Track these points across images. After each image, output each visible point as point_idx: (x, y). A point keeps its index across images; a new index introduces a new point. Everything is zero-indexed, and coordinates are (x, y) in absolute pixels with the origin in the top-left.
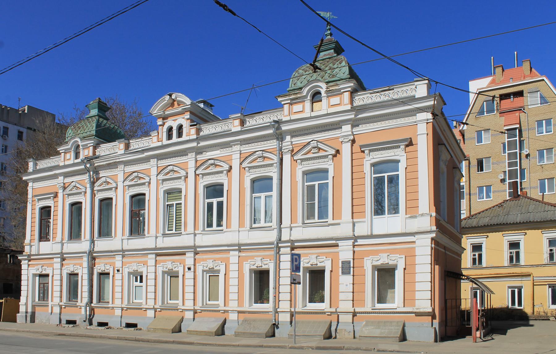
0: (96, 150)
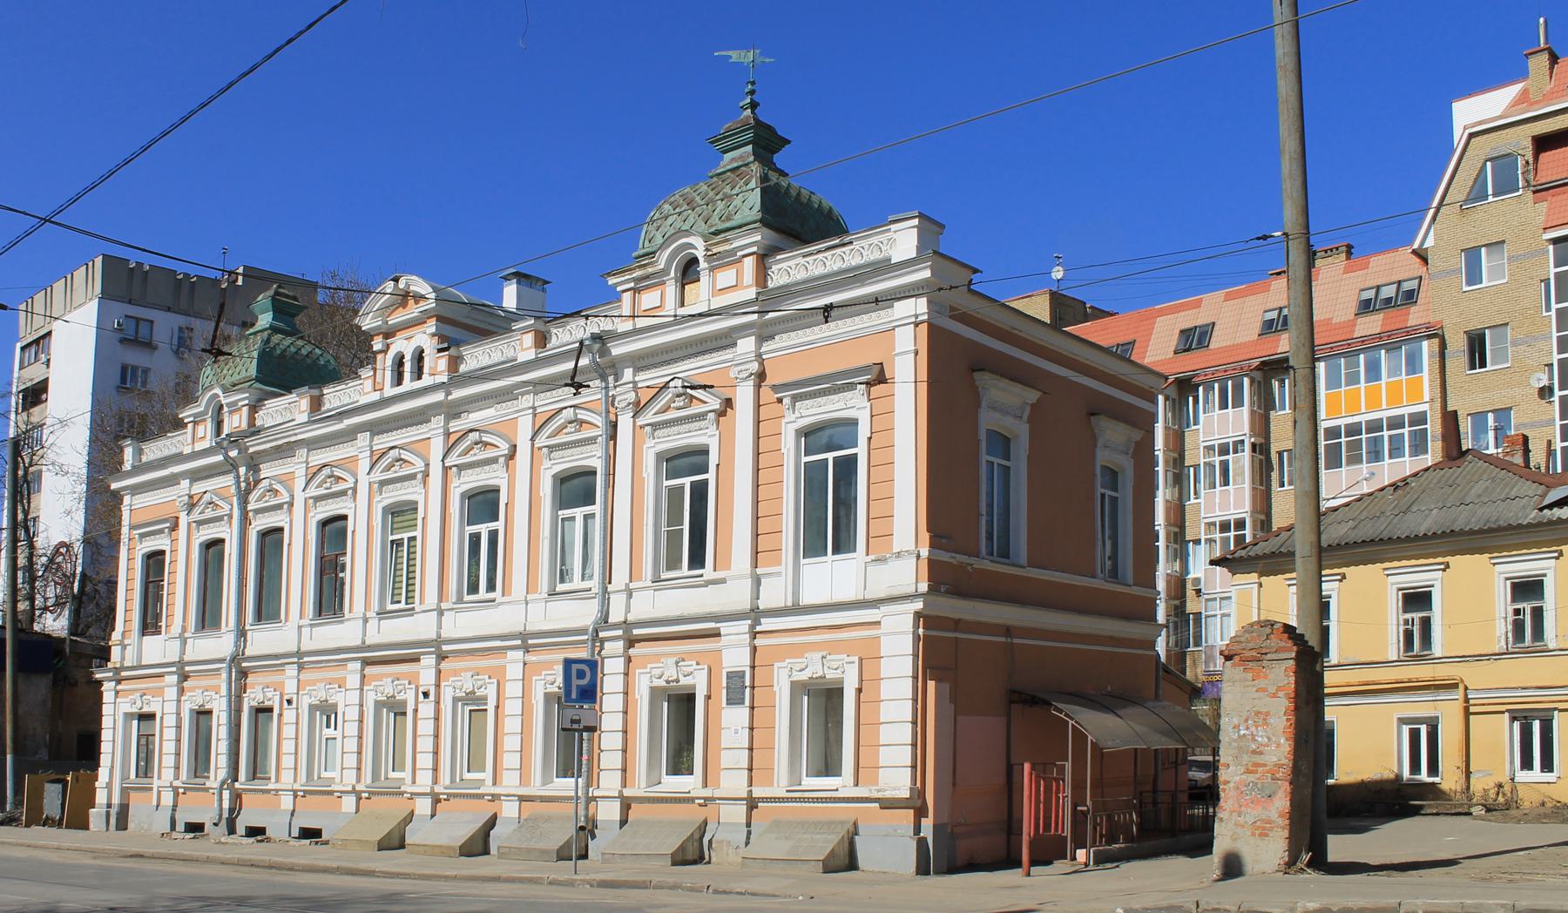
0: (256, 415)
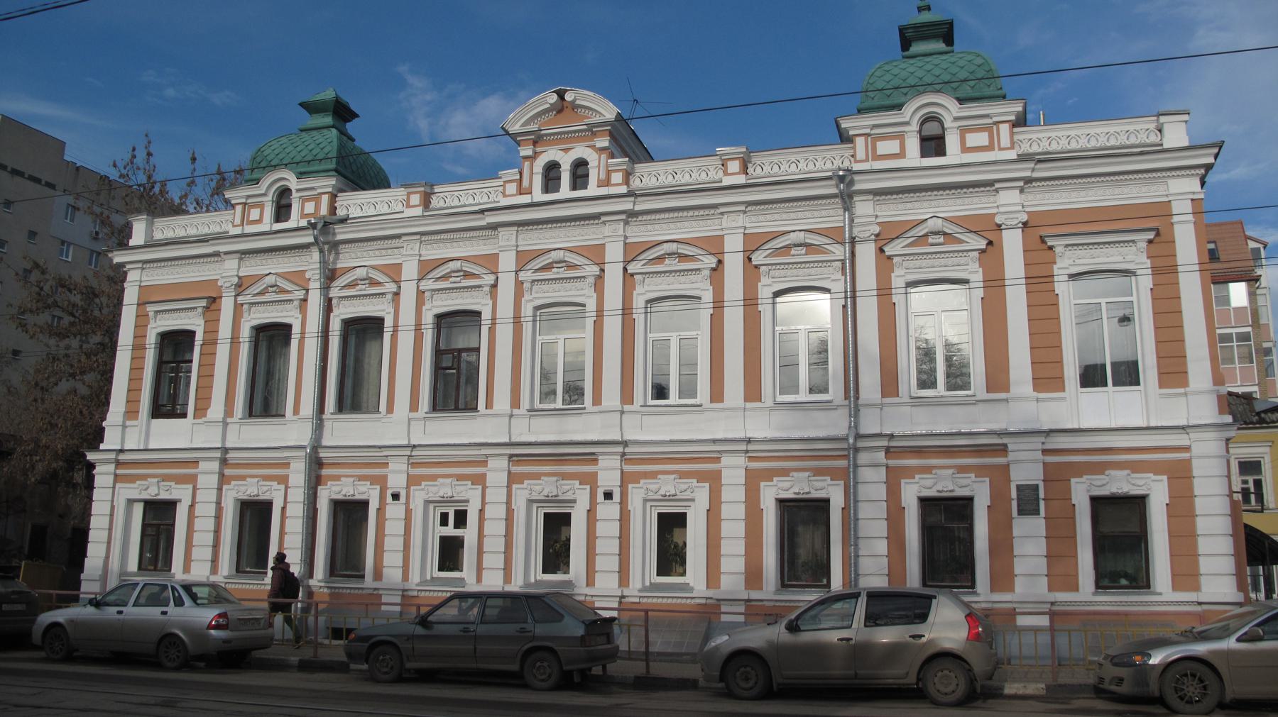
0: (336, 204)
